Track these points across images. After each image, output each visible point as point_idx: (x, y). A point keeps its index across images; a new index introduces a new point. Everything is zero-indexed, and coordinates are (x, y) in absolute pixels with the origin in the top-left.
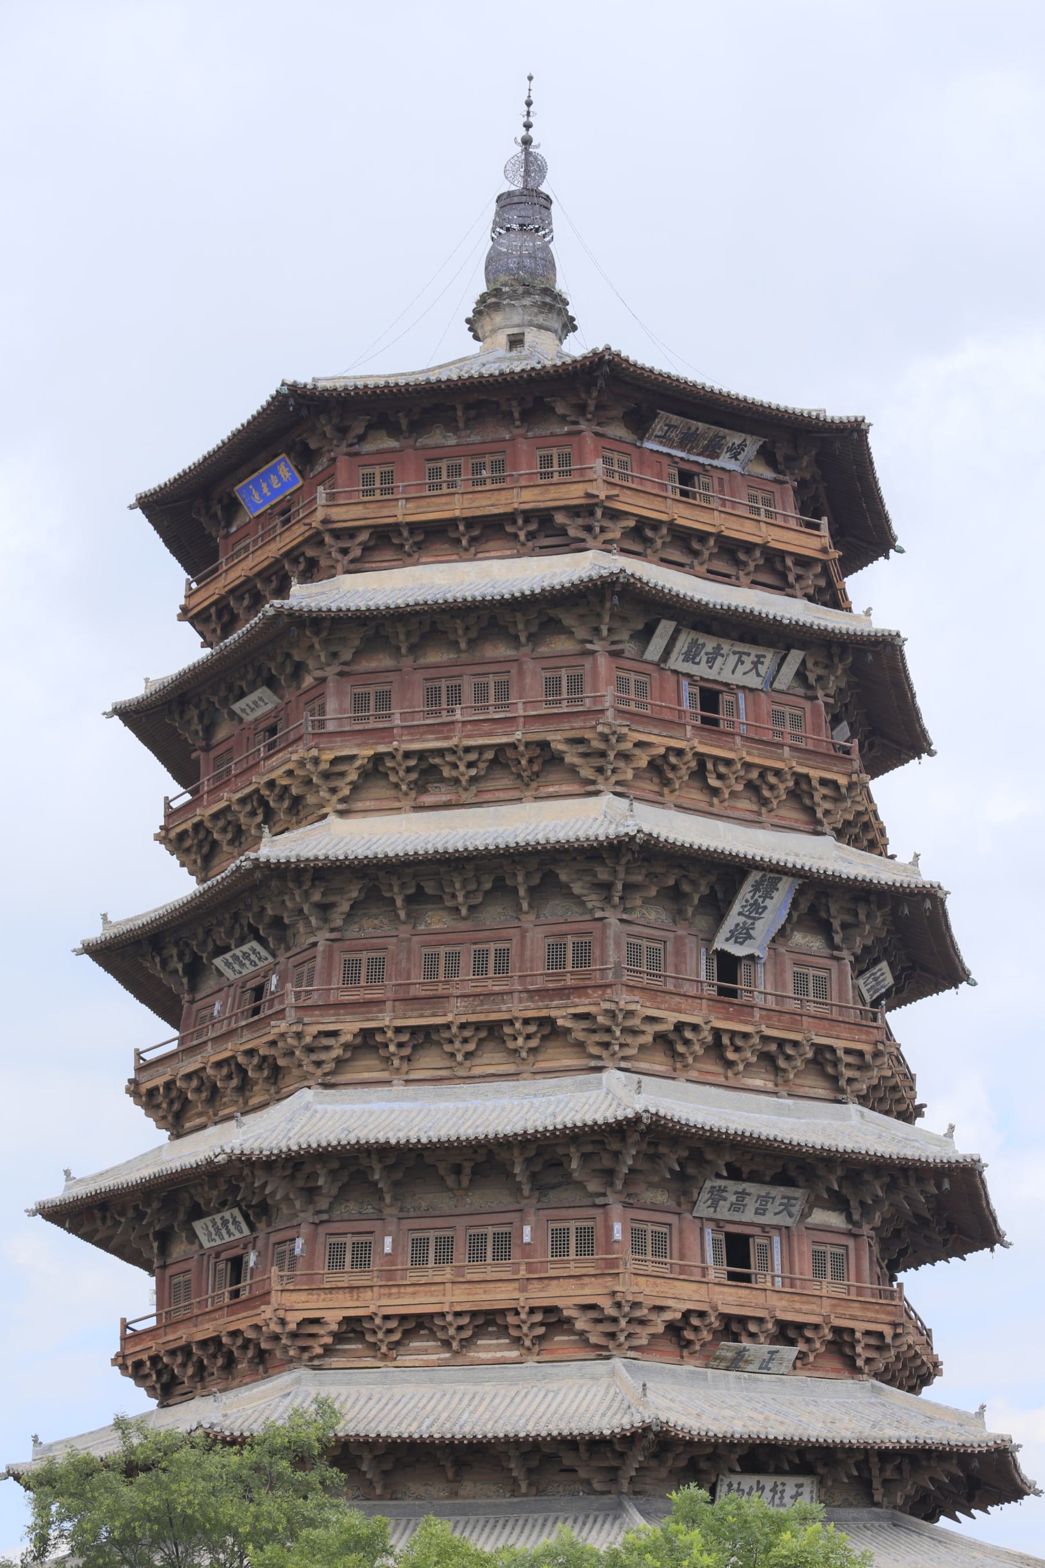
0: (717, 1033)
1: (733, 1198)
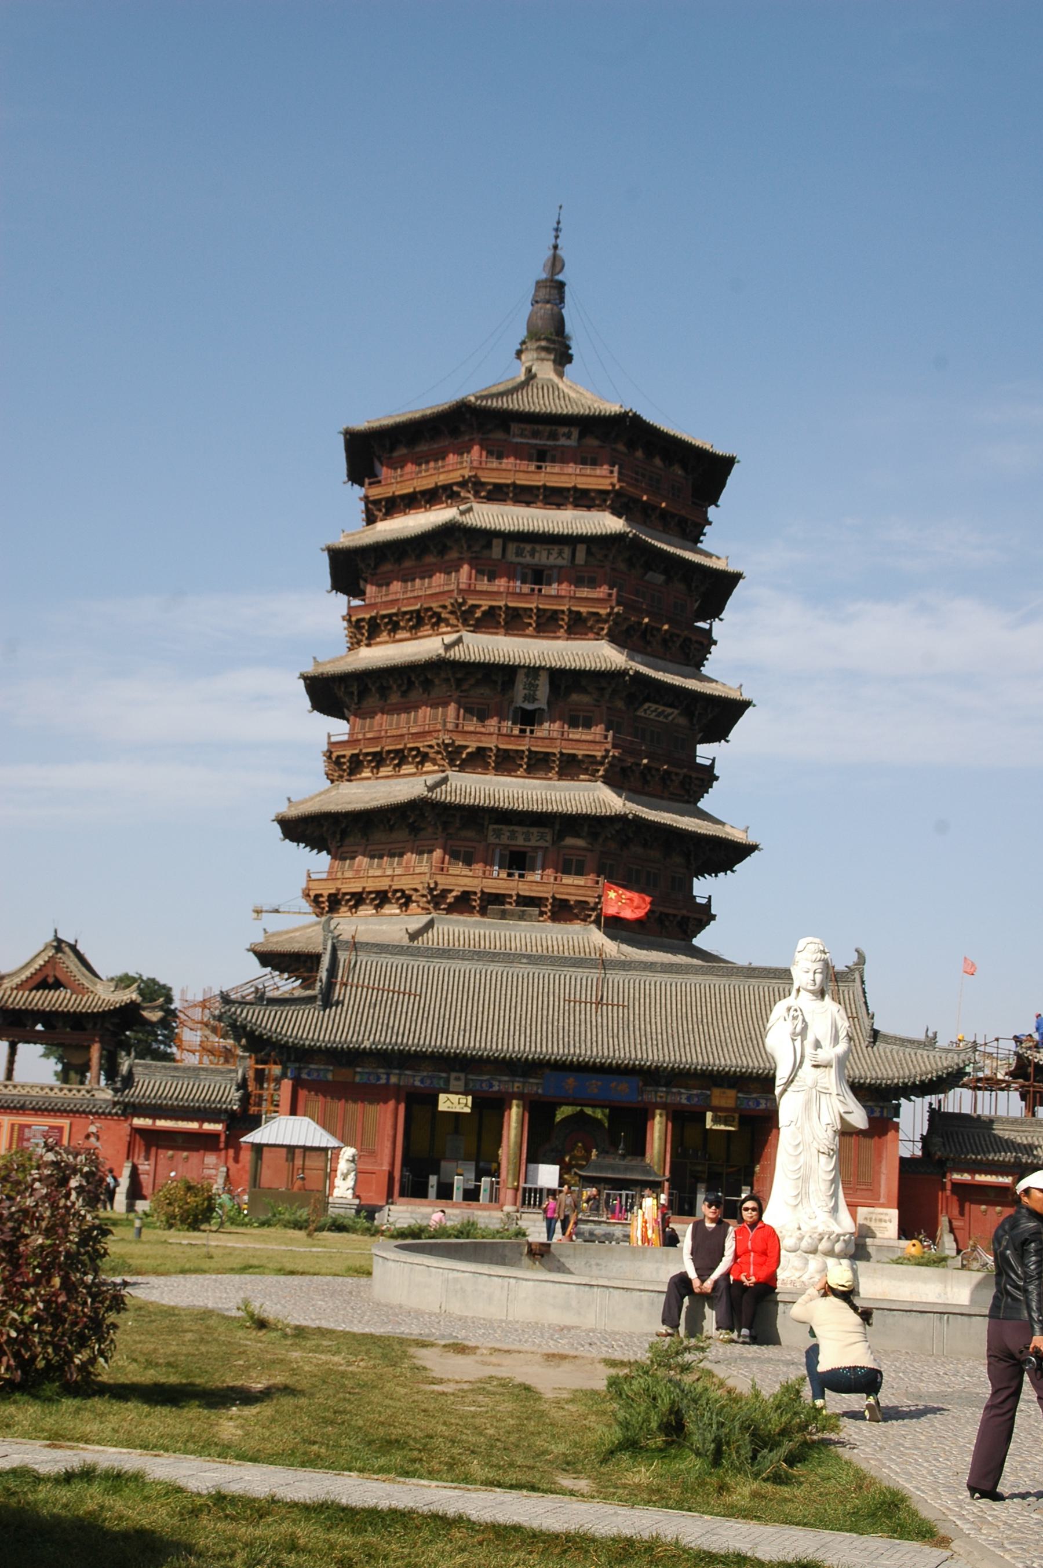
0: (506, 751)
1: (508, 834)
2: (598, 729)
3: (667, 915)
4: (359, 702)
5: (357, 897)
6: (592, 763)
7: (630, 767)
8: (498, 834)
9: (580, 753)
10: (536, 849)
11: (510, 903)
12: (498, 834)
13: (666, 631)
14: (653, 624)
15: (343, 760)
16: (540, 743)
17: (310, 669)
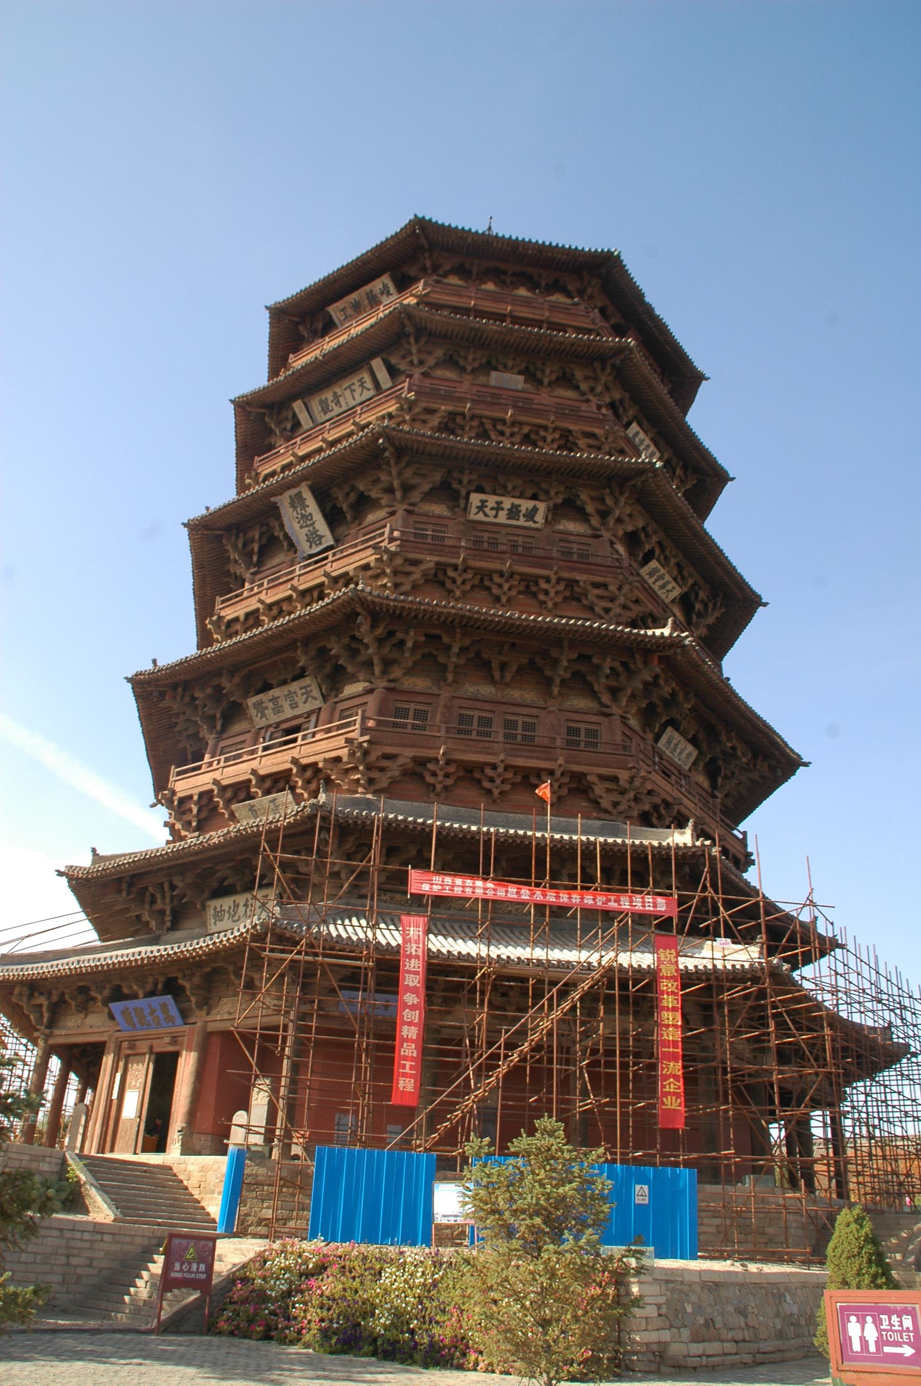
1: (271, 705)
14: (486, 413)
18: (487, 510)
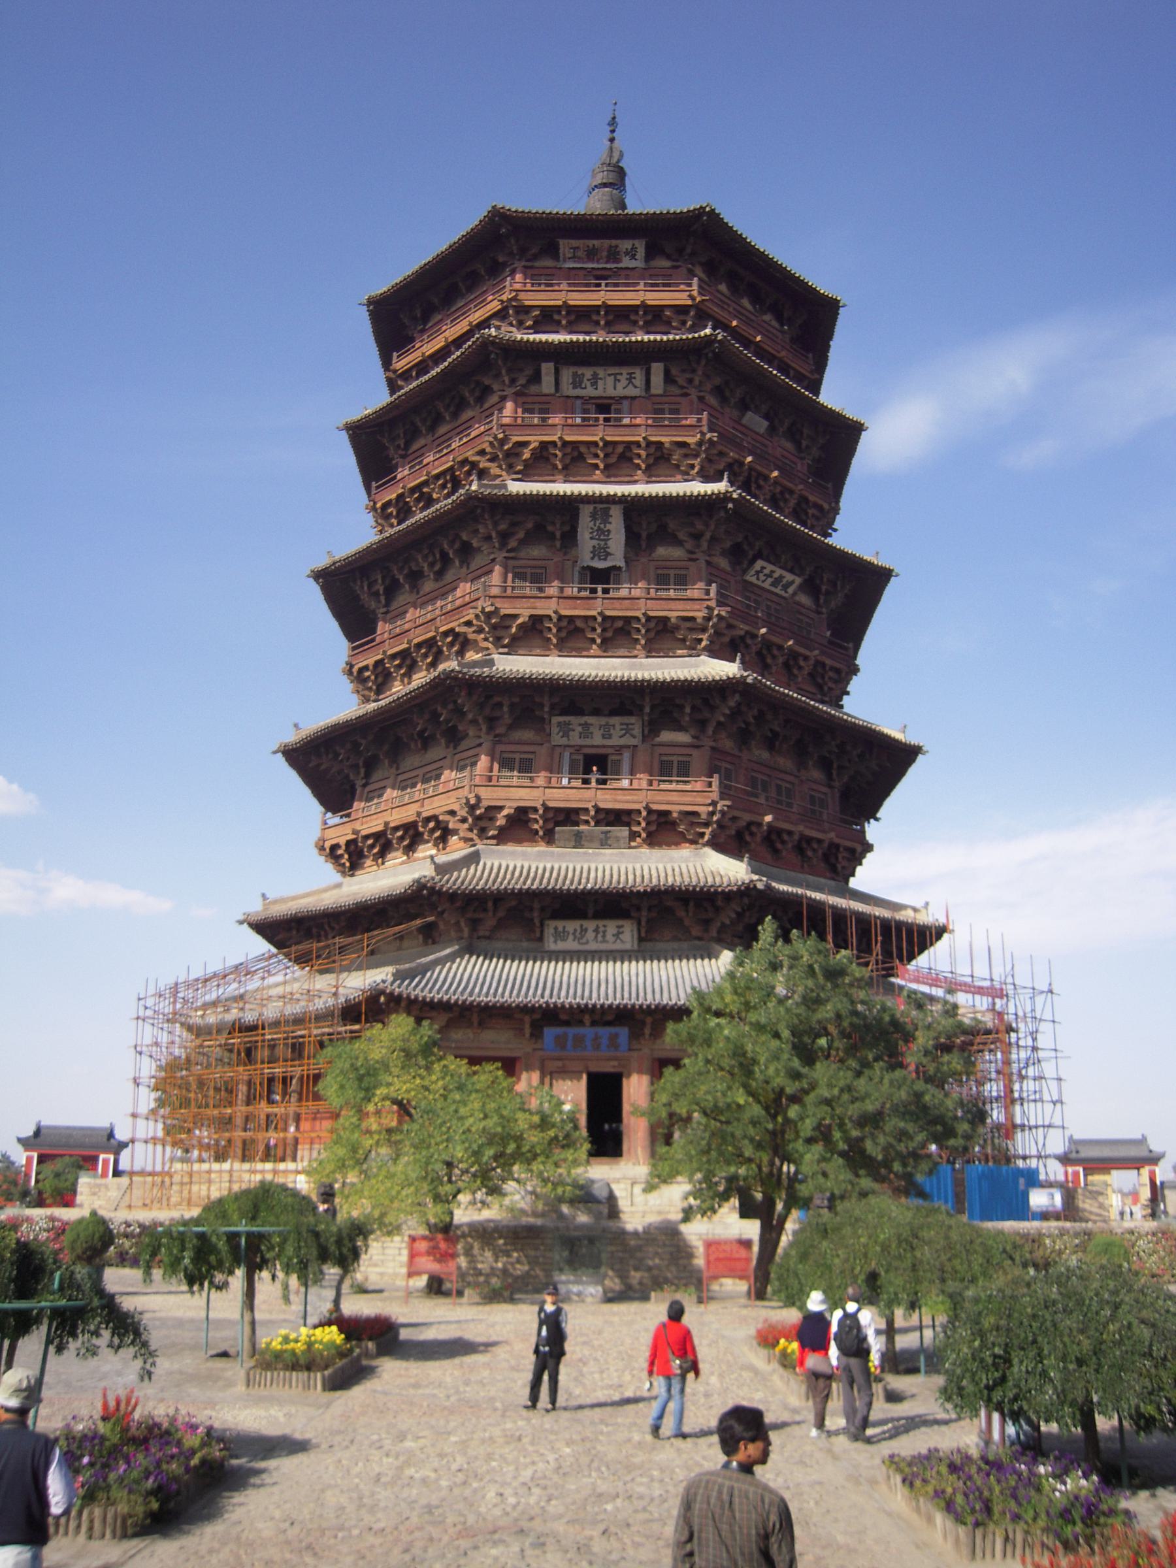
0: (571, 619)
1: (580, 729)
2: (695, 590)
3: (809, 840)
4: (387, 604)
5: (382, 841)
6: (691, 630)
7: (742, 638)
8: (566, 730)
9: (673, 615)
10: (620, 749)
11: (587, 822)
12: (566, 730)
13: (776, 482)
14: (759, 468)
15: (367, 674)
16: (617, 604)
17: (322, 562)
18: (762, 577)
